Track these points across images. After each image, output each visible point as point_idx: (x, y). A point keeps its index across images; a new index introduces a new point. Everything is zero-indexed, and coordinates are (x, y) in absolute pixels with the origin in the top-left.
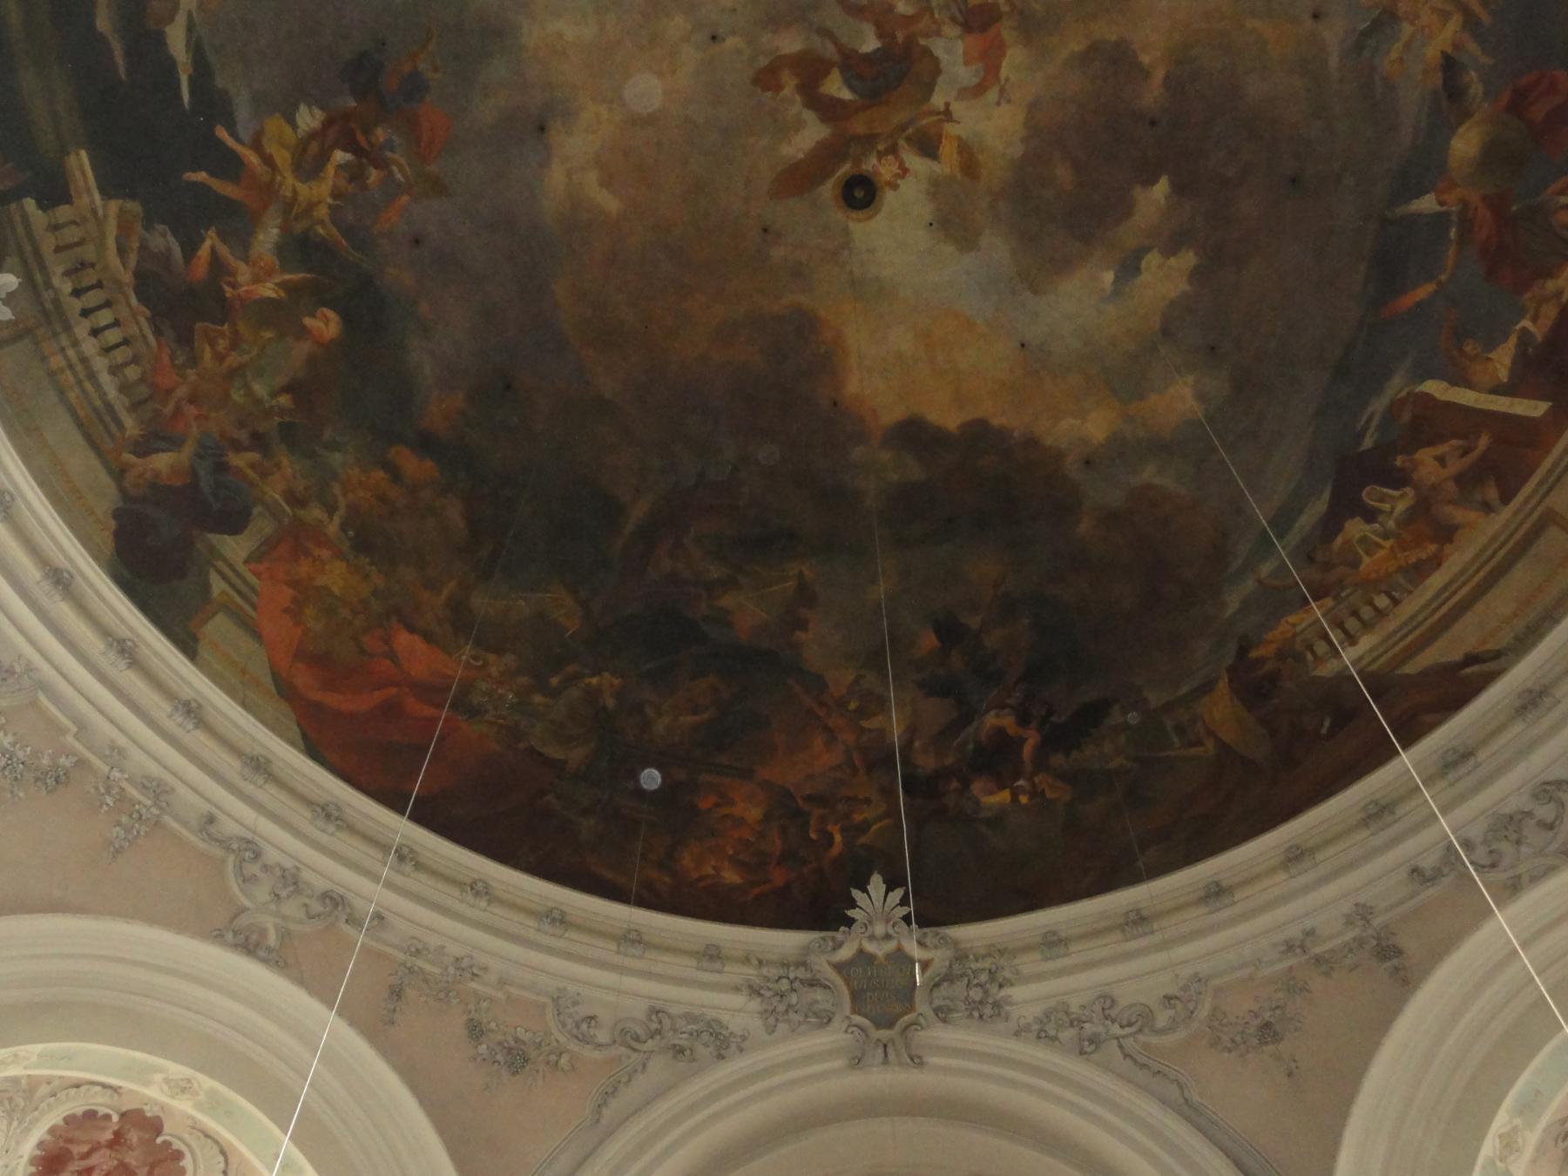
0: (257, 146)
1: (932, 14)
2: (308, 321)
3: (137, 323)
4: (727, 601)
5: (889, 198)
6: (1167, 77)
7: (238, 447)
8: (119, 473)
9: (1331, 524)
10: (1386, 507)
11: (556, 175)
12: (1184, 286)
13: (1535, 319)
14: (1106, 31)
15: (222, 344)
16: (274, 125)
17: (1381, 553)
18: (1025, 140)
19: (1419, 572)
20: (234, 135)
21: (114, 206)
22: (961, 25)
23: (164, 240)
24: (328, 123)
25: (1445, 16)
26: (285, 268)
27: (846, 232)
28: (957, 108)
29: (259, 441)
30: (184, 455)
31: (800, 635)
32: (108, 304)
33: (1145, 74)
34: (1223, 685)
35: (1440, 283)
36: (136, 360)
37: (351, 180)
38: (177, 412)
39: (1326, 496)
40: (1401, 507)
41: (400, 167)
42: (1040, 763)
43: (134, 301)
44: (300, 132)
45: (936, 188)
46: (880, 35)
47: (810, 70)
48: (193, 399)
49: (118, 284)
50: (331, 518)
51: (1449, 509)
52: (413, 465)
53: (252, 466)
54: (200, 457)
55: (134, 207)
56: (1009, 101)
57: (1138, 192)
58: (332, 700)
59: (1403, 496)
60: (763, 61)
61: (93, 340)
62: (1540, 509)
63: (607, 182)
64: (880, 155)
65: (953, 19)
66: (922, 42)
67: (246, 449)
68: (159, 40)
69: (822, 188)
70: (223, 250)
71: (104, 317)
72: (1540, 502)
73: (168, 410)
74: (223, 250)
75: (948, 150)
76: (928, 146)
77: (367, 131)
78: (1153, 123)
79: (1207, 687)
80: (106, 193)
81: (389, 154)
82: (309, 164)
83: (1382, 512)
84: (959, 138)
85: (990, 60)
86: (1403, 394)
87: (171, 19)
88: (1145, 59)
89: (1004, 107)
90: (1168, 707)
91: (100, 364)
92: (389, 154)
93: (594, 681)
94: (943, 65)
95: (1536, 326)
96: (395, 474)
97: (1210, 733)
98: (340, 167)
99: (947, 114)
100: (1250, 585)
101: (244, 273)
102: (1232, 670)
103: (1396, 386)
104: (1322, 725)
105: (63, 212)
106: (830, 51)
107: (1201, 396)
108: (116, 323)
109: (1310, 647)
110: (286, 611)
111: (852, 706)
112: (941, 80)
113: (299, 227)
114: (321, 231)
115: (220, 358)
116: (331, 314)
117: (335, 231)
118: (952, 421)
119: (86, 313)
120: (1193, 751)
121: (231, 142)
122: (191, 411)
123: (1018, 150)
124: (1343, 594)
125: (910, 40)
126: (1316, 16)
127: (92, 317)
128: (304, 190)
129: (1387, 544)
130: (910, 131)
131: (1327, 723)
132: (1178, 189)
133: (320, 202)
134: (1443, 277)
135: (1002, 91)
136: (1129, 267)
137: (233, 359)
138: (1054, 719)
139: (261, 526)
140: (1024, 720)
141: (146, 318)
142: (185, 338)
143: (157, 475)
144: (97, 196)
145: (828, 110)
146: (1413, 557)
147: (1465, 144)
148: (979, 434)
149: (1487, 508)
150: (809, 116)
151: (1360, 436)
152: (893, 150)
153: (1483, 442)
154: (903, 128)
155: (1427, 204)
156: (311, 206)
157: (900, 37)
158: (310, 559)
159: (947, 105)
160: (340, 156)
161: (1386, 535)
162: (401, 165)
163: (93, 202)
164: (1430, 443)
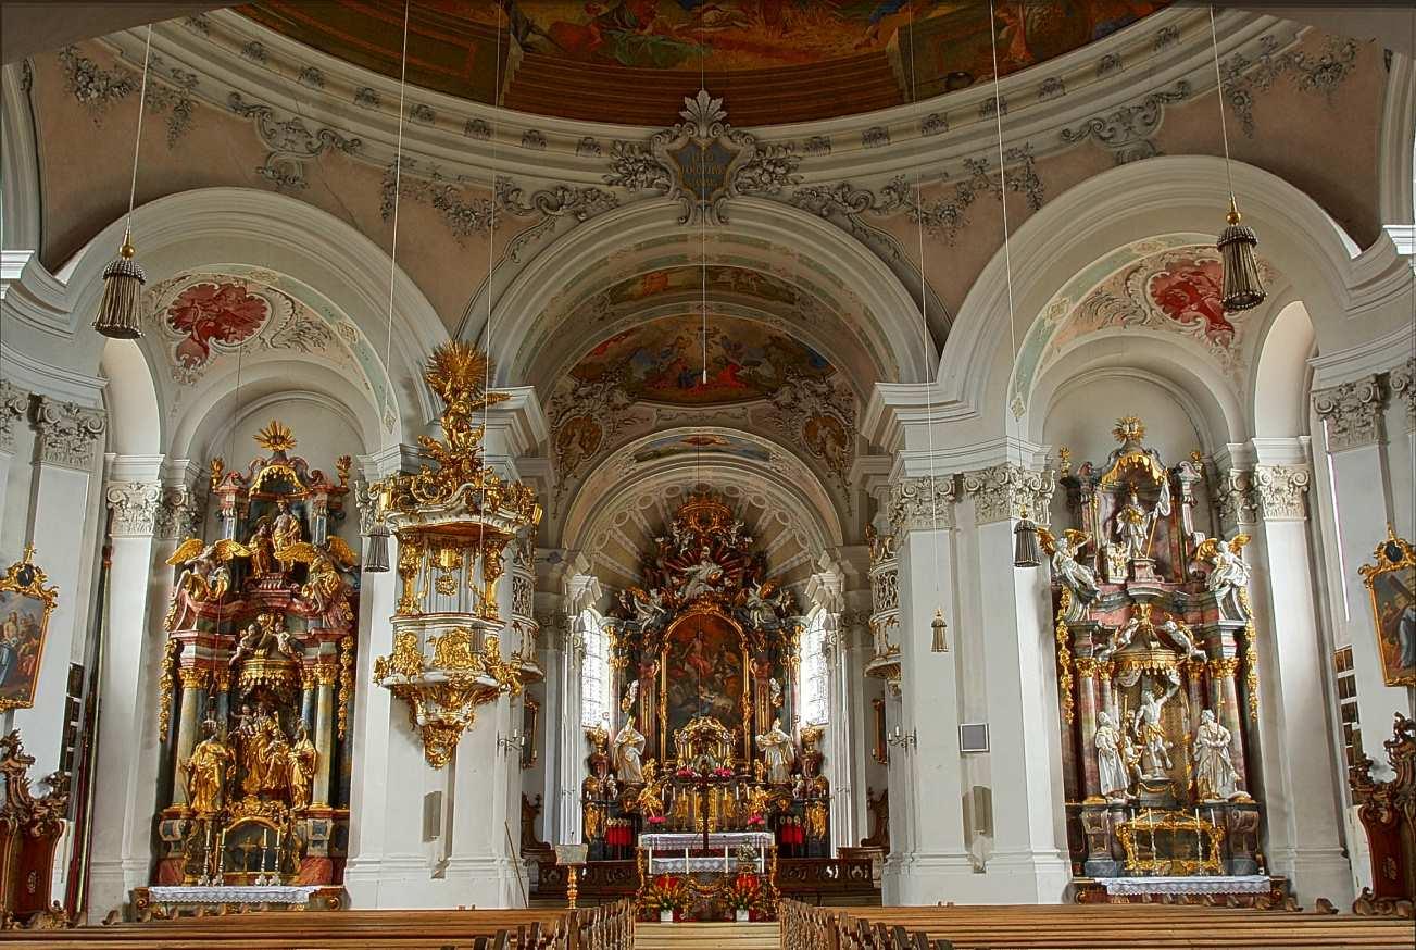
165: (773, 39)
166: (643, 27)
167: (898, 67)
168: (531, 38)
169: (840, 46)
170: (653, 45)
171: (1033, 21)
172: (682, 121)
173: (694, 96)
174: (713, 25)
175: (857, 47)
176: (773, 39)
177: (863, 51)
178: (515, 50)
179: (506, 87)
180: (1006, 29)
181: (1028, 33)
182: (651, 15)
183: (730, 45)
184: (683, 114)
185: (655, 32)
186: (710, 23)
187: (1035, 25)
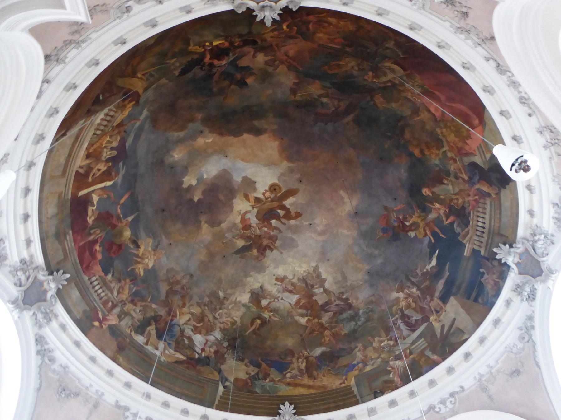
0: (426, 235)
1: (258, 228)
2: (431, 194)
3: (473, 218)
4: (321, 92)
5: (267, 188)
6: (200, 222)
7: (463, 179)
8: (498, 194)
9: (123, 142)
10: (109, 153)
11: (355, 202)
12: (184, 179)
13: (93, 210)
14: (217, 229)
15: (455, 201)
16: (420, 236)
17: (105, 142)
18: (233, 203)
19: (91, 145)
20: (430, 239)
21: (464, 242)
22: (252, 226)
23: (457, 229)
24: (408, 231)
25: (143, 254)
26: (432, 208)
27: (279, 180)
28: (250, 208)
29: (457, 178)
30: (477, 186)
31: (296, 81)
32: (478, 226)
33: (206, 222)
34: (140, 91)
35: (119, 205)
36: (479, 212)
37: (407, 218)
38: (475, 195)
39: (127, 148)
40: (105, 155)
41: (394, 215)
42: (203, 55)
43: (471, 223)
44: (415, 232)
45: (255, 190)
46: (271, 224)
47: (288, 216)
48: (469, 195)
49: (472, 227)
50: (446, 151)
51: (91, 161)
52: (417, 152)
53: (462, 173)
54: (474, 184)
55: (460, 238)
56: (238, 211)
57: (202, 197)
58: (470, 113)
59: (105, 157)
60: (299, 219)
61: (486, 222)
62: (67, 175)
63: (342, 198)
64: (270, 197)
65: (253, 227)
66: (261, 222)
67: (461, 177)
68: (437, 264)
69: (285, 190)
70: (444, 219)
71: (480, 224)
72: (68, 178)
73: (477, 197)
74: (444, 219)
75: (252, 199)
76: (257, 200)
77: (399, 226)
78: (202, 212)
79: (146, 90)
80: (464, 246)
81: (395, 219)
82: (414, 226)
83: (109, 151)
84: (250, 202)
85: (243, 220)
86: (117, 178)
87: (433, 267)
88: (206, 225)
89: (239, 210)
90: (158, 80)
91: (487, 216)
92: (395, 219)
93: (375, 80)
94: (255, 218)
95: (90, 209)
96: (422, 151)
97: (141, 78)
98: (409, 222)
99: (253, 207)
100: (142, 118)
101: (442, 212)
102: (139, 96)
103: (119, 179)
104: (102, 96)
105: (476, 248)
106: (284, 220)
107: (172, 156)
108: (478, 221)
109: (116, 112)
110: (471, 138)
111: (277, 63)
112: (255, 214)
113: (423, 214)
114: (418, 211)
115: (457, 199)
116: (424, 193)
117: (415, 209)
118: (246, 136)
119: (484, 228)
120: (145, 72)
121: (432, 238)
122: (471, 193)
123: (234, 201)
124: (111, 129)
125: (263, 222)
126: (171, 244)
127: (483, 221)
128: (419, 221)
129: (103, 146)
130: (262, 203)
131: (101, 98)
132: (191, 200)
133: (416, 217)
134: (119, 206)
135: (240, 213)
136: (200, 180)
137: (454, 197)
138: (200, 66)
139: (467, 160)
140: (211, 65)
141: (470, 217)
142: (463, 208)
143: (488, 188)
144: (467, 246)
145: (283, 208)
146: (95, 146)
147: (127, 233)
148: (237, 133)
149: (81, 167)
150: (288, 206)
151: (123, 164)
152: (266, 199)
153: (90, 179)
154: (264, 204)
155: (130, 219)
156: (419, 217)
157: (266, 223)
158: (457, 145)
159: (253, 209)
160: (408, 224)
161: (105, 147)
162: (394, 216)
163: (469, 245)
164: (104, 172)
165: (311, 382)
166: (266, 379)
167: (355, 390)
168: (227, 384)
169: (334, 384)
170: (269, 386)
171: (401, 370)
172: (280, 414)
173: (284, 404)
174: (290, 378)
175: (341, 384)
176: (311, 382)
177: (343, 385)
178: (221, 389)
179: (216, 402)
180: (392, 373)
181: (400, 373)
182: (269, 375)
183: (296, 385)
184: (280, 411)
185: (270, 381)
186: (289, 377)
187: (402, 371)
